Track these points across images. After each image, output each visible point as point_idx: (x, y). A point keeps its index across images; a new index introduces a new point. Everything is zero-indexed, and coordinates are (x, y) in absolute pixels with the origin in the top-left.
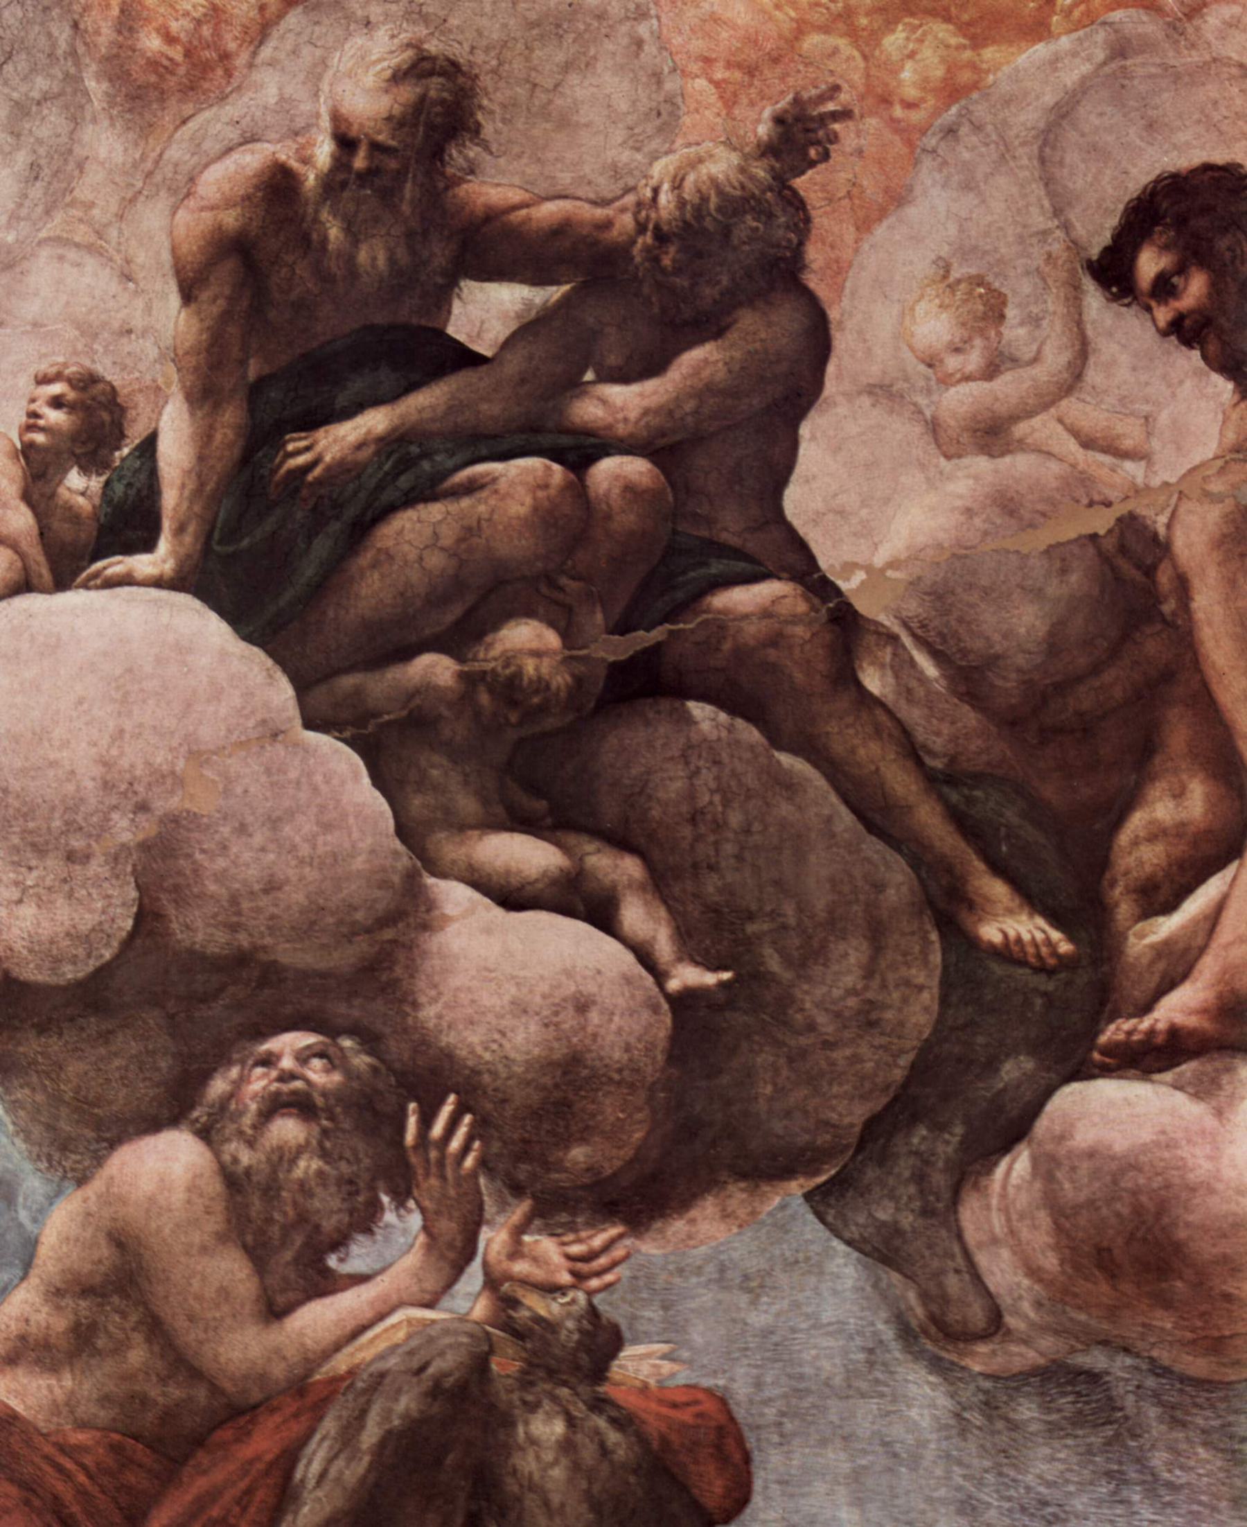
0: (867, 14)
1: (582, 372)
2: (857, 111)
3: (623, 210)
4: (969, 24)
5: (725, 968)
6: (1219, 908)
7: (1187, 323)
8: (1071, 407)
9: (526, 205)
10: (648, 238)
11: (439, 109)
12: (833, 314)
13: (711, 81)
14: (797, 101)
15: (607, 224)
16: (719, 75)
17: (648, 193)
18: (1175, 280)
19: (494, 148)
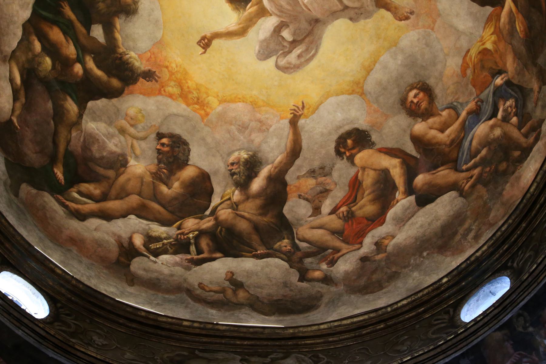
0: (175, 77)
1: (93, 54)
2: (158, 83)
3: (122, 49)
4: (183, 94)
5: (19, 127)
7: (160, 151)
8: (135, 142)
9: (118, 32)
10: (120, 56)
11: (129, 8)
12: (123, 95)
13: (150, 56)
14: (155, 72)
15: (119, 48)
16: (152, 56)
17: (127, 53)
18: (165, 146)
19: (126, 21)
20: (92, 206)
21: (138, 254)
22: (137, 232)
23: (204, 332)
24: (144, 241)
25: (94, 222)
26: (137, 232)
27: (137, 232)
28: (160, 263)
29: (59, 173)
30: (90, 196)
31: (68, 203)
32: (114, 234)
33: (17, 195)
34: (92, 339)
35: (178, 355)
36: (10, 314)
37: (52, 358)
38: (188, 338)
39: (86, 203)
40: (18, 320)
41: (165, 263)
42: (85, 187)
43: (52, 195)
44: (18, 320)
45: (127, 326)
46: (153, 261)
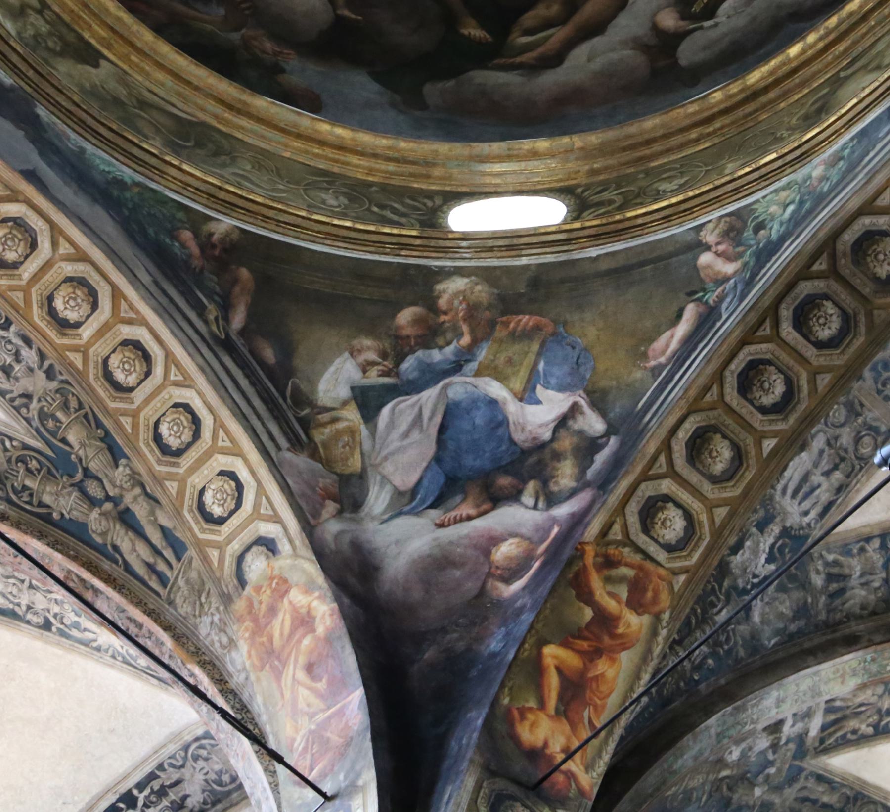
6: (551, 36)
20: (559, 35)
21: (680, 36)
22: (659, 9)
23: (832, 37)
24: (678, 12)
25: (580, 54)
26: (659, 9)
27: (658, 12)
28: (724, 19)
29: (473, 31)
30: (548, 24)
31: (518, 60)
32: (624, 43)
33: (424, 107)
34: (659, 191)
35: (813, 104)
36: (491, 249)
37: (599, 256)
38: (815, 67)
39: (547, 38)
40: (510, 248)
41: (732, 13)
42: (529, 19)
43: (486, 68)
44: (510, 248)
45: (709, 134)
46: (711, 27)
